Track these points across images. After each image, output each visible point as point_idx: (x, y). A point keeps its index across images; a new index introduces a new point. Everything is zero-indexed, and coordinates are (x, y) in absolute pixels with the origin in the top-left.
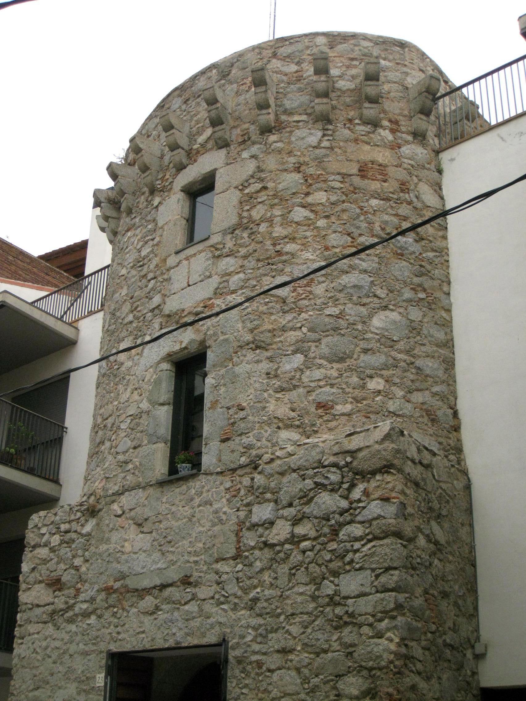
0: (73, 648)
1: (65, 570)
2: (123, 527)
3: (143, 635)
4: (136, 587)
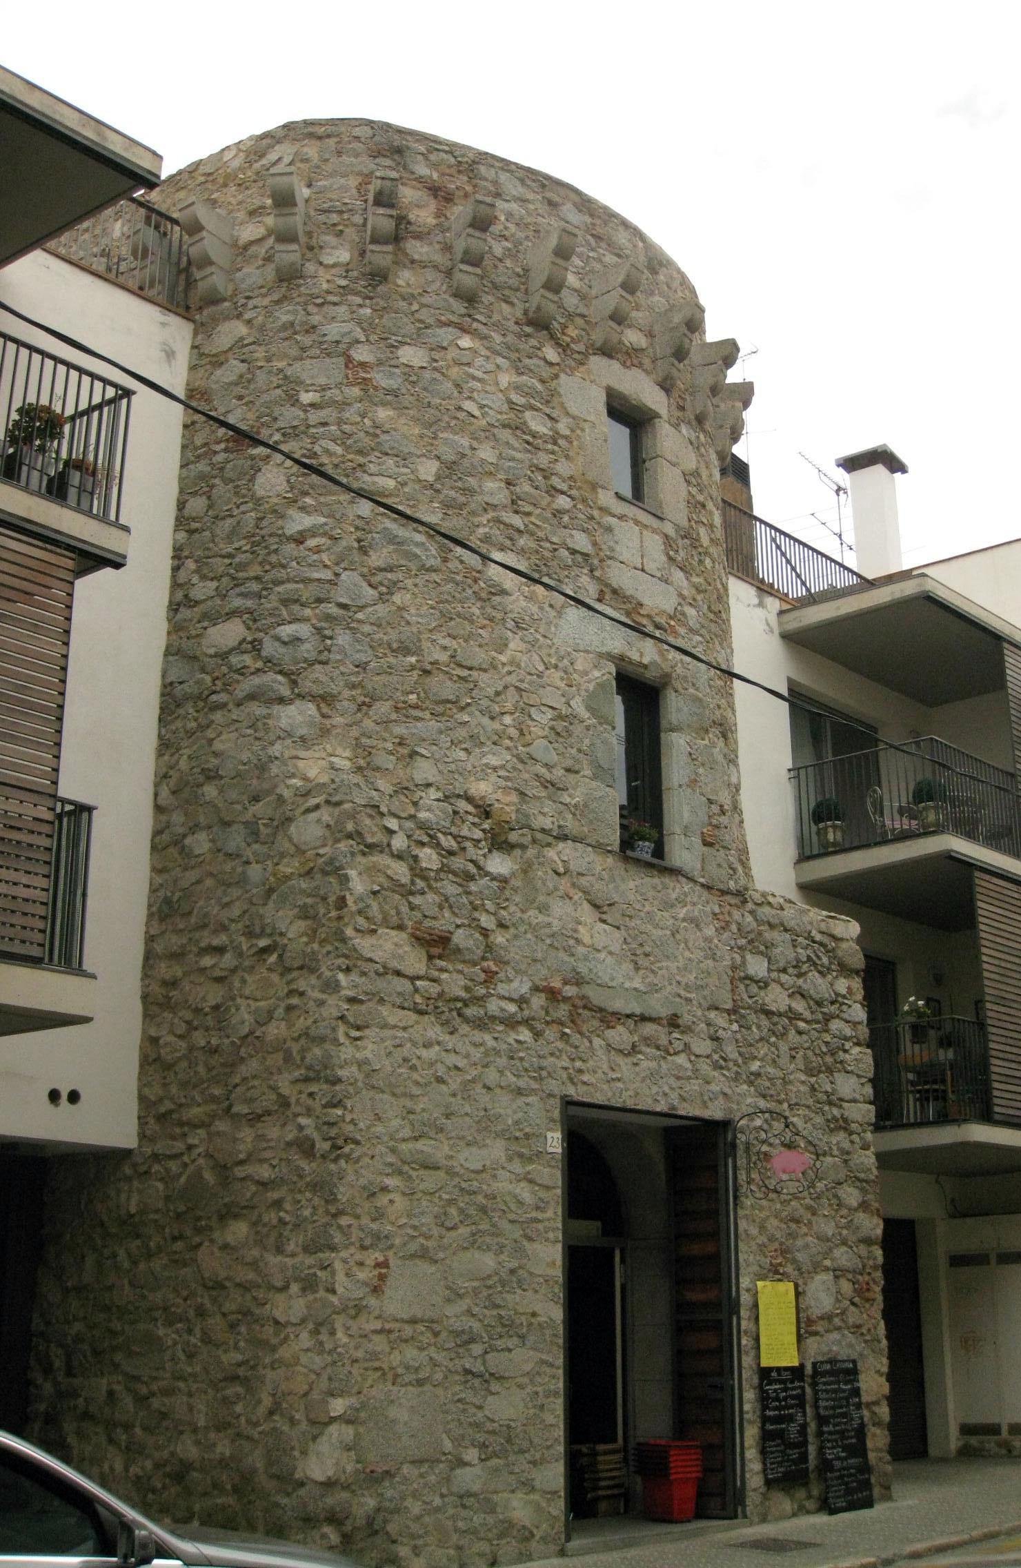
0: (492, 1076)
3: (620, 1085)
4: (602, 1005)
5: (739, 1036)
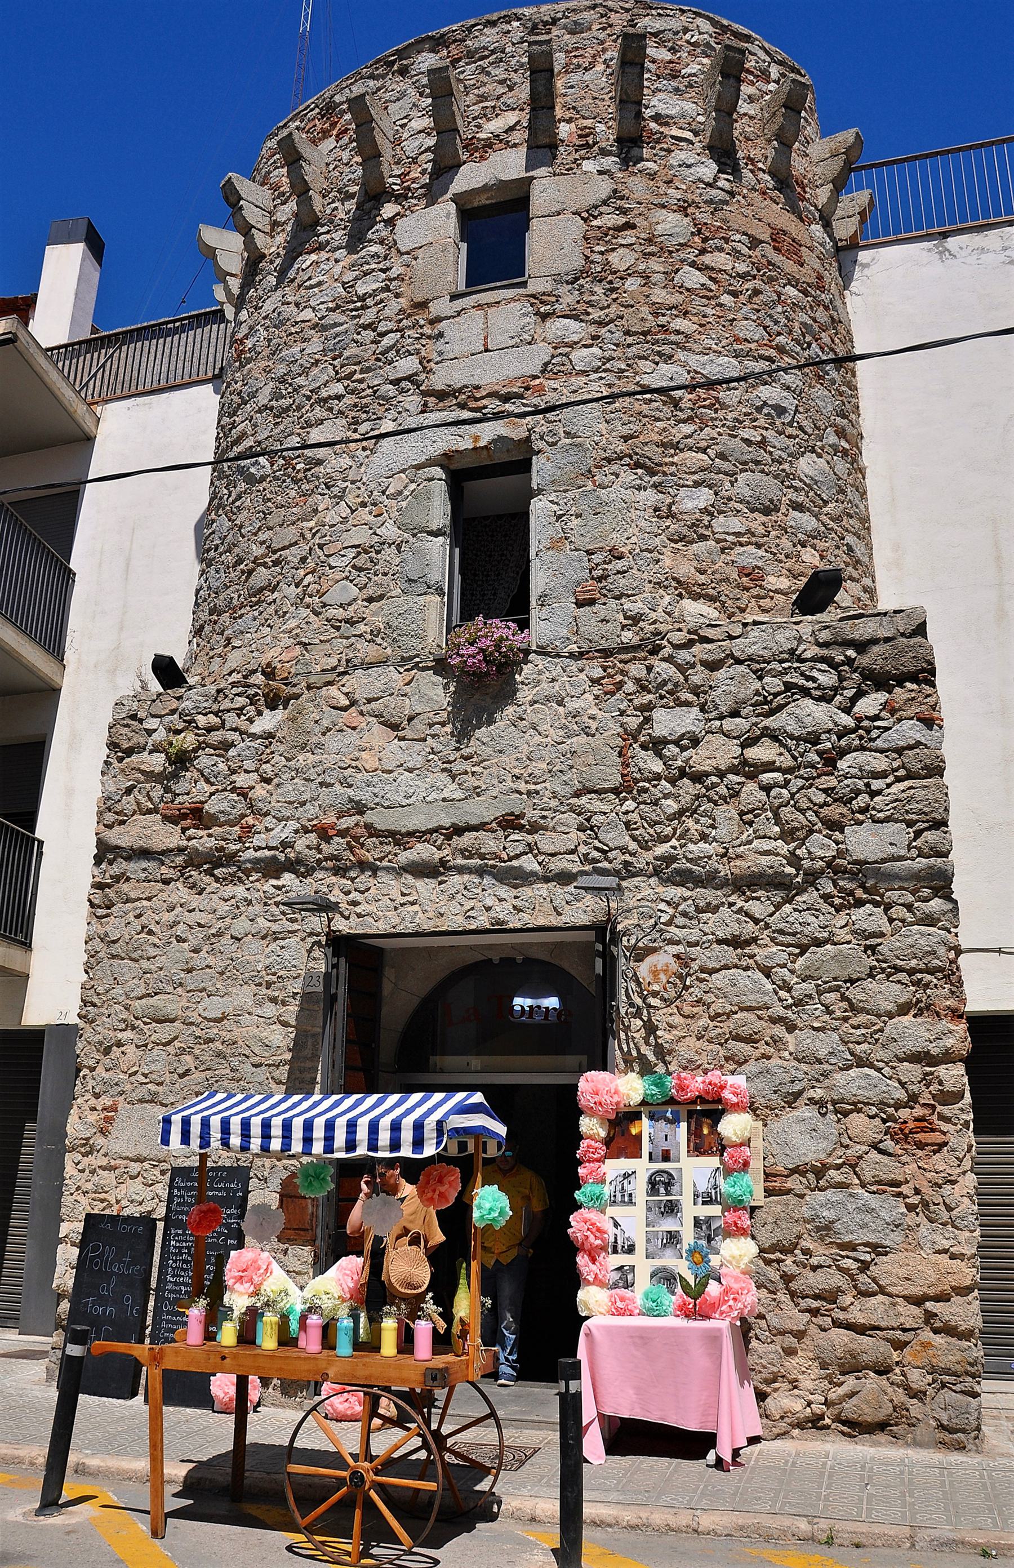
0: (241, 925)
1: (212, 794)
2: (354, 728)
3: (416, 908)
4: (392, 828)
5: (634, 817)
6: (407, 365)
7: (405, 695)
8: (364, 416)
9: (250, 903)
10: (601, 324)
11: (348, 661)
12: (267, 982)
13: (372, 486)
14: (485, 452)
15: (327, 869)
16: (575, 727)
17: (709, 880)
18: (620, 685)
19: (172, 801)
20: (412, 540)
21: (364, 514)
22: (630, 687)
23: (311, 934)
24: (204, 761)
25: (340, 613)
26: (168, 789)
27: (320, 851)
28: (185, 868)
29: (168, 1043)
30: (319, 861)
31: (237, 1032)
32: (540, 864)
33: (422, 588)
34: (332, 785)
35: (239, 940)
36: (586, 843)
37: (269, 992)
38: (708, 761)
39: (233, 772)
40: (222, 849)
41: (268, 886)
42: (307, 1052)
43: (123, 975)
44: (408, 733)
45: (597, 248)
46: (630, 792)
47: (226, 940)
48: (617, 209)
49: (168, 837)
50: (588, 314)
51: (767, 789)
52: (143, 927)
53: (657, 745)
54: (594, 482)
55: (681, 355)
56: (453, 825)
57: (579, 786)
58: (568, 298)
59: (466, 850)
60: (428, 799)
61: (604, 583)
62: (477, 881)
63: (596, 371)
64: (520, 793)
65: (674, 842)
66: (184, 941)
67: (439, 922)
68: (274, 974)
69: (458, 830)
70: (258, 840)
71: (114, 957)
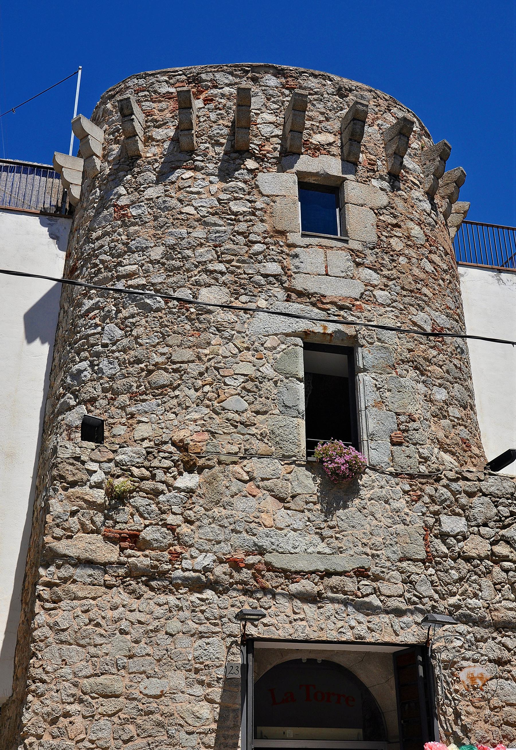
0: (174, 625)
1: (146, 526)
2: (254, 496)
3: (304, 623)
4: (285, 567)
5: (435, 578)
6: (273, 268)
7: (288, 480)
8: (242, 291)
9: (181, 609)
10: (388, 278)
11: (246, 450)
12: (196, 669)
13: (254, 338)
14: (329, 337)
15: (238, 590)
16: (398, 519)
17: (480, 622)
18: (420, 497)
19: (113, 527)
20: (285, 380)
21: (248, 355)
22: (427, 499)
23: (230, 636)
24: (139, 501)
25: (237, 417)
26: (107, 517)
27: (231, 577)
28: (126, 578)
29: (113, 715)
30: (231, 584)
31: (172, 707)
32: (382, 601)
33: (295, 414)
34: (241, 532)
35: (172, 635)
36: (409, 592)
37: (198, 676)
38: (474, 551)
39: (163, 512)
40: (156, 567)
41: (195, 597)
42: (230, 723)
43: (71, 658)
44: (291, 505)
45: (384, 233)
46: (431, 563)
47: (161, 635)
48: (391, 214)
49: (109, 553)
50: (382, 271)
51: (507, 571)
52: (91, 620)
53: (443, 536)
54: (397, 372)
55: (427, 309)
56: (326, 570)
57: (401, 555)
58: (370, 259)
59: (335, 587)
60: (309, 551)
61: (405, 434)
62: (343, 608)
63: (388, 306)
64: (367, 555)
65: (458, 597)
66: (127, 633)
67: (321, 634)
68: (202, 663)
69: (329, 574)
70: (185, 564)
71: (62, 642)
